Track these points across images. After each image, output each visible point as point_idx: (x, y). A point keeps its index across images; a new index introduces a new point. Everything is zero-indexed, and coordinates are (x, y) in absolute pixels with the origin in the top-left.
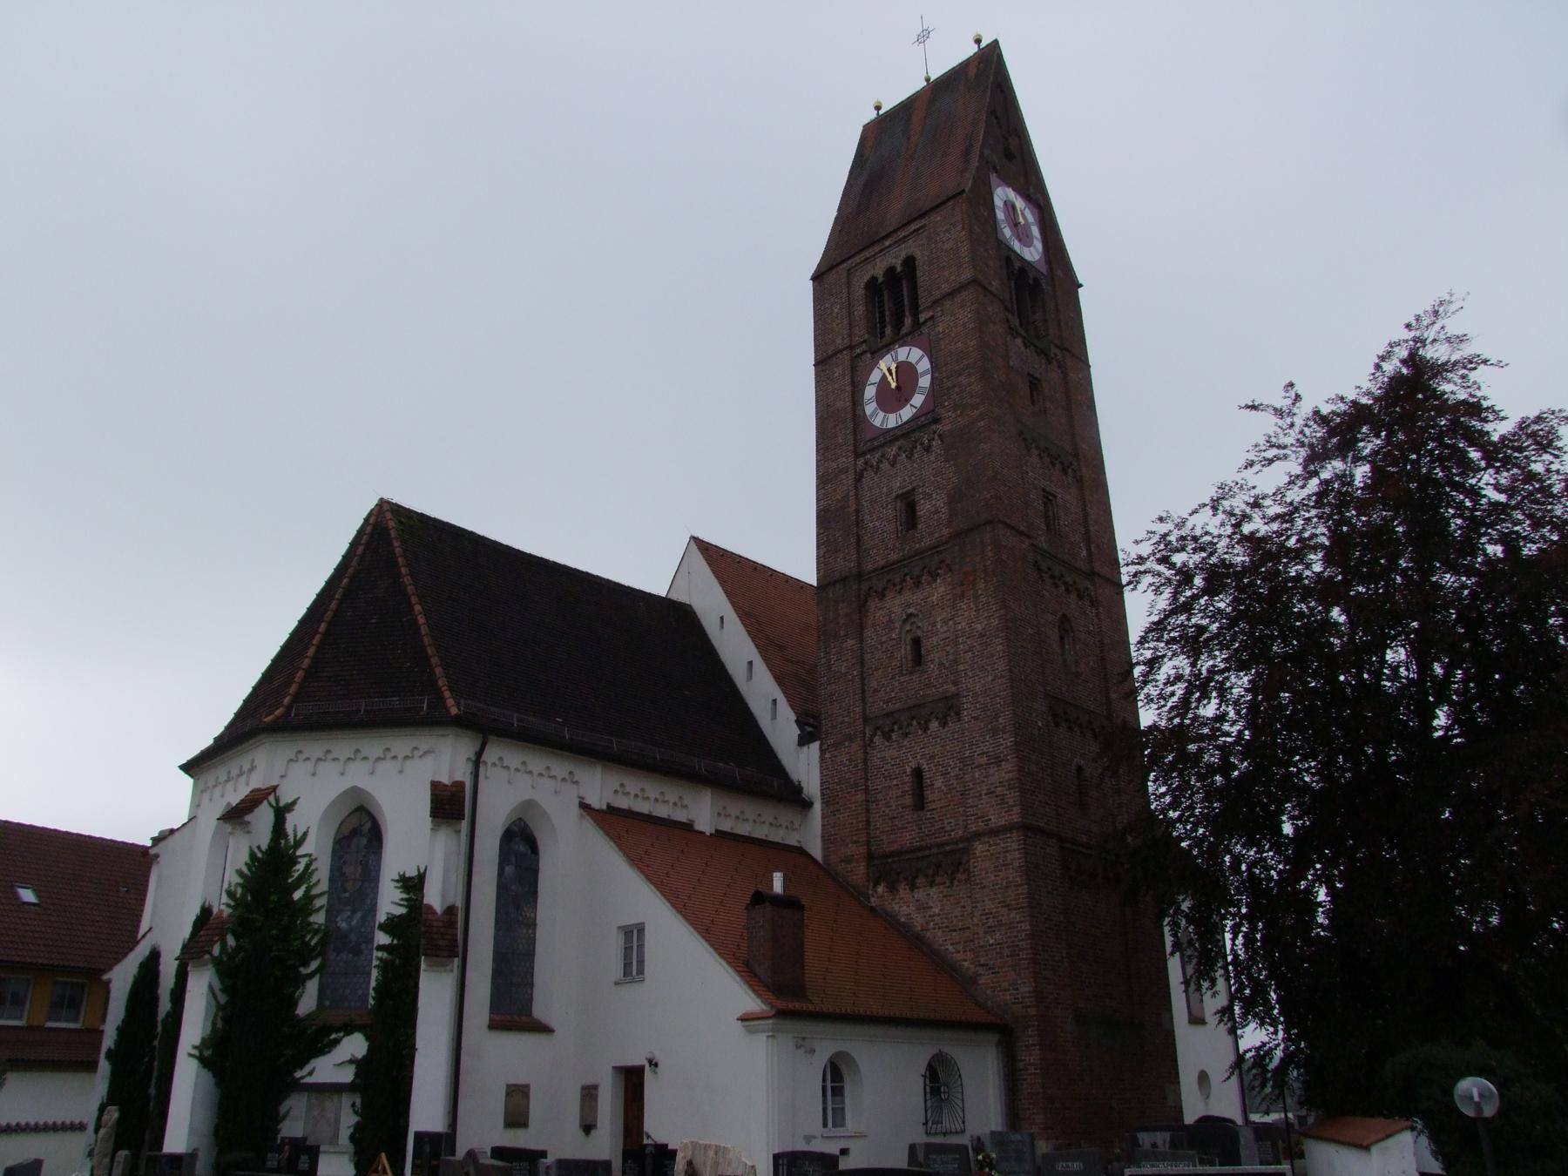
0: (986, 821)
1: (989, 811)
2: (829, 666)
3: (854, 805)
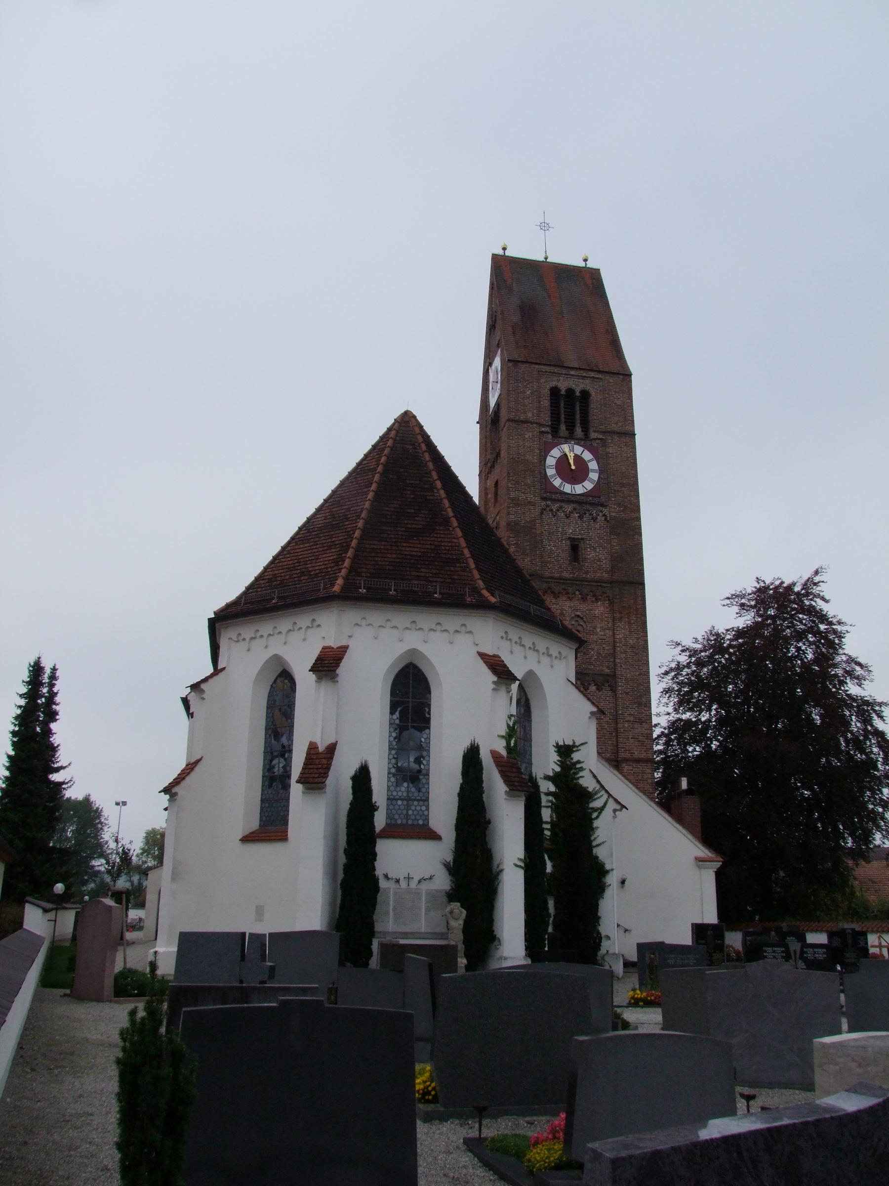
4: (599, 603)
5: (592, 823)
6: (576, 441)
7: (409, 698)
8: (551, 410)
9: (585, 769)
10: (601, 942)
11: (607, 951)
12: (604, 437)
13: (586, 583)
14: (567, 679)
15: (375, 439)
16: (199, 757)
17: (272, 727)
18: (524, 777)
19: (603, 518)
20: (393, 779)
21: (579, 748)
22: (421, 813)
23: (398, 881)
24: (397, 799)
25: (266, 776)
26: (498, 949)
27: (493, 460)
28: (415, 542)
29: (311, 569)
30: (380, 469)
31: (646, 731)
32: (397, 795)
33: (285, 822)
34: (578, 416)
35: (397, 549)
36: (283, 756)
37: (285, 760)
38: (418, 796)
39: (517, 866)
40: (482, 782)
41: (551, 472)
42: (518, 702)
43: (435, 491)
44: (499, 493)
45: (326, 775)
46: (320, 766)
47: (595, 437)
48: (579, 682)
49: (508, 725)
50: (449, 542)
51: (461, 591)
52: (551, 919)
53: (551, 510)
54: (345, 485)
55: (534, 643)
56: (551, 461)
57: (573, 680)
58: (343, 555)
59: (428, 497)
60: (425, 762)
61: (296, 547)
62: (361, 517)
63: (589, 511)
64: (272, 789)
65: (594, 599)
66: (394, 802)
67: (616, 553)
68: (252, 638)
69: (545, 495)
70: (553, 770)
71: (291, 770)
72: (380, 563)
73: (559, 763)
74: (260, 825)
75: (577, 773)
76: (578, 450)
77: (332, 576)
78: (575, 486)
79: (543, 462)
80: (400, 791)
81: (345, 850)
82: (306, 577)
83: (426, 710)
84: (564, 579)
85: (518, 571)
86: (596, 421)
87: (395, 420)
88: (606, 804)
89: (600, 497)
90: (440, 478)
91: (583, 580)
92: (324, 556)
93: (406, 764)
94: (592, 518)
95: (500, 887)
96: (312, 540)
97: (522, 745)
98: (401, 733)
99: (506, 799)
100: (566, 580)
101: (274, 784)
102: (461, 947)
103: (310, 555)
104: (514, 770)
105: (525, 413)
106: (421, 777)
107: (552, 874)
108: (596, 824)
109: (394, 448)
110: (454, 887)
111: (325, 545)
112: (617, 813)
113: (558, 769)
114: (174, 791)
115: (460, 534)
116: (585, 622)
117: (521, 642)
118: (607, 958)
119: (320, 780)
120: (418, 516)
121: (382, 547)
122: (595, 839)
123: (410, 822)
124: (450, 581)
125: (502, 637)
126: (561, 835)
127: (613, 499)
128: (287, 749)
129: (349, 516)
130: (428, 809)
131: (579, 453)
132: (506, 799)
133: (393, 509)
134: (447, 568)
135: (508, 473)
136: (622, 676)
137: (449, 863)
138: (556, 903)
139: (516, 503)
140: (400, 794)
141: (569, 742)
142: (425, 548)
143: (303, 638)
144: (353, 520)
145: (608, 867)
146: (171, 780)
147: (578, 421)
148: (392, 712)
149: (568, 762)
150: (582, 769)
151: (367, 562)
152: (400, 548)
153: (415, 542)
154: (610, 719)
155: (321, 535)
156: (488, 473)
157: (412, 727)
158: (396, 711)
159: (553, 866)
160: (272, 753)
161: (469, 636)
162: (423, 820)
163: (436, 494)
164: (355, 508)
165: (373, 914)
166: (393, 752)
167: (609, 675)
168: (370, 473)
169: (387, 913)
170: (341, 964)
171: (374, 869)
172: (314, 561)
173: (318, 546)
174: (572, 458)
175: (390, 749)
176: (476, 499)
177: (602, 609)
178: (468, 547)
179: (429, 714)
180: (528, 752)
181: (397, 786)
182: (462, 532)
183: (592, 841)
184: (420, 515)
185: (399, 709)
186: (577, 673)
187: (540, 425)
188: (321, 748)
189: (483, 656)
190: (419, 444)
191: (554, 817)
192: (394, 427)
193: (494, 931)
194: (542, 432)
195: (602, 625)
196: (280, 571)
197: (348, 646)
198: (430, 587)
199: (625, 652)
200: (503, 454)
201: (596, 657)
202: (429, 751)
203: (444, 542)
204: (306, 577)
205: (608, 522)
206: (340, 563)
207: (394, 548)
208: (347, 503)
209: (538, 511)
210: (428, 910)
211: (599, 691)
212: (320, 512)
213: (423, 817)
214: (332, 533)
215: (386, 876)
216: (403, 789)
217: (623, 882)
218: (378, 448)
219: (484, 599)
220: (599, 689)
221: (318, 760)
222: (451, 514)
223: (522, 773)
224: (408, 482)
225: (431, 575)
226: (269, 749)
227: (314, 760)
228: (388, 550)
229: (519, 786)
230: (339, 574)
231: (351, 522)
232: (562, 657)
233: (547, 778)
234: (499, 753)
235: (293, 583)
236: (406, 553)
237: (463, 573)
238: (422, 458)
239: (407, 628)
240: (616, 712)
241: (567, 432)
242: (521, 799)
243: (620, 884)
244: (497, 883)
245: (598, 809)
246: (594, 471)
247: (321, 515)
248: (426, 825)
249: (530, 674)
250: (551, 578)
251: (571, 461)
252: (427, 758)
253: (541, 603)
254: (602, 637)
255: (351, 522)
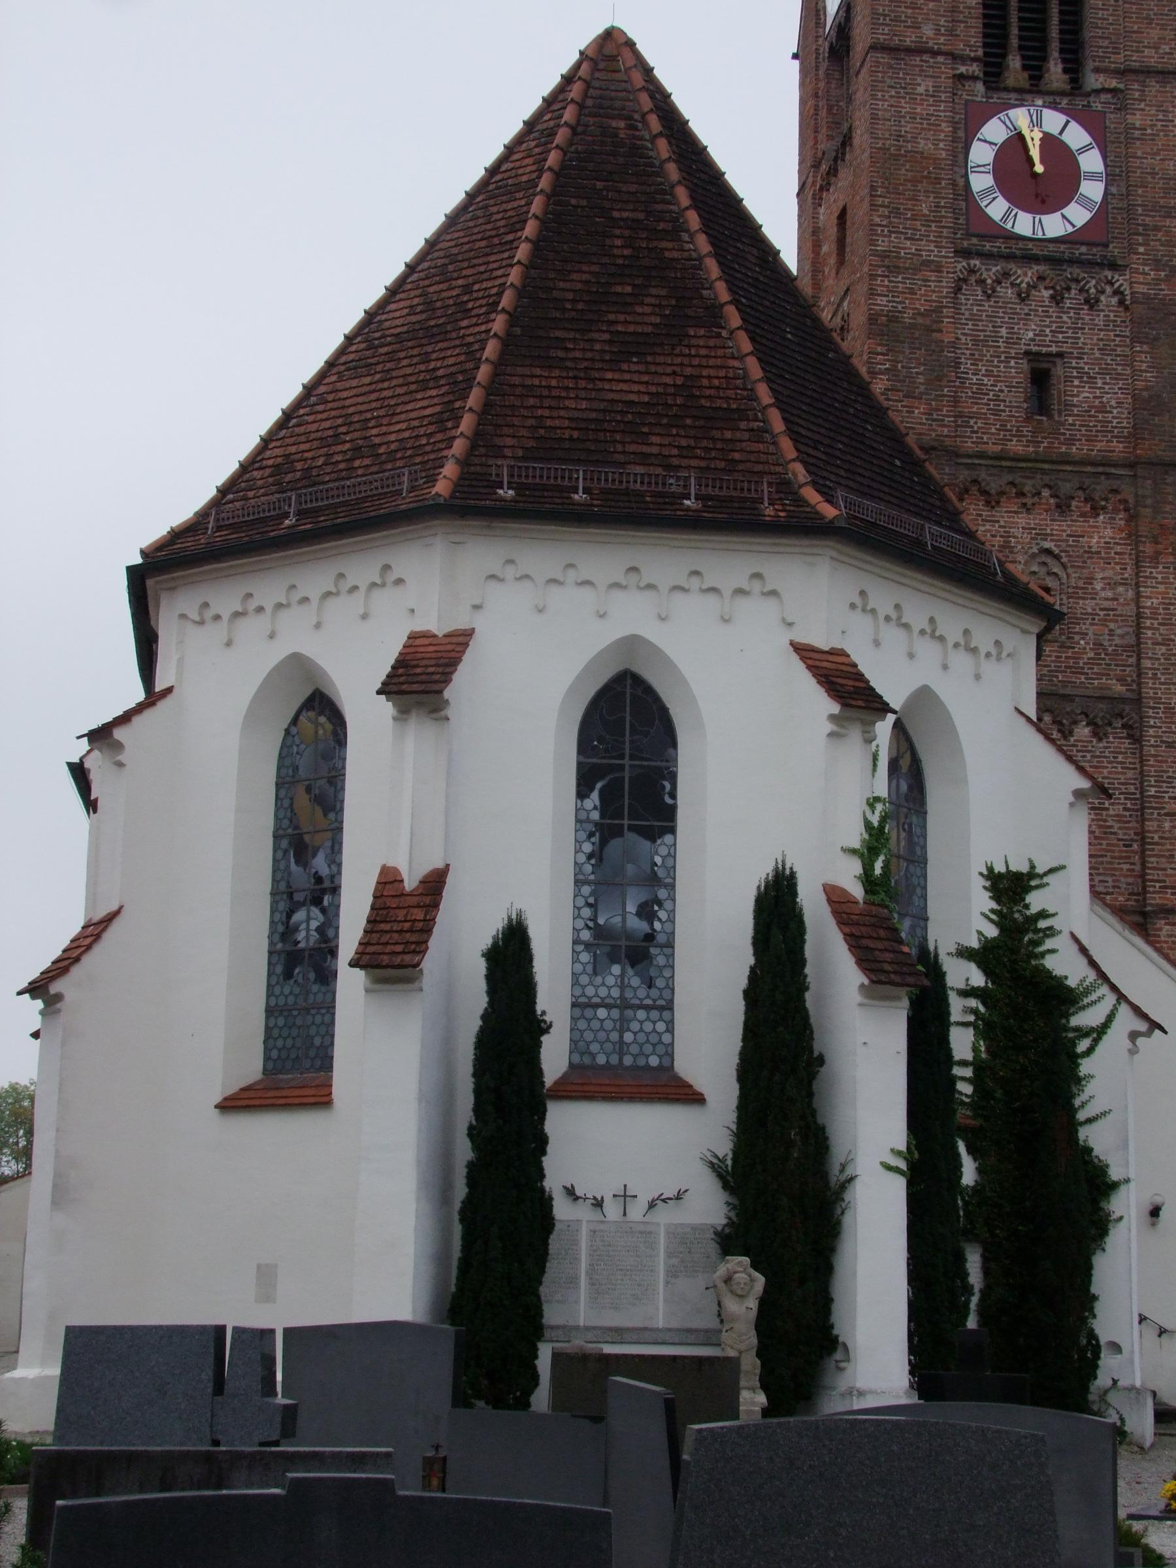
4: (1101, 517)
5: (1078, 1065)
6: (1049, 99)
7: (622, 757)
8: (985, 16)
9: (1060, 932)
10: (1099, 1358)
11: (1115, 1382)
12: (1121, 86)
13: (1069, 468)
14: (1016, 709)
15: (530, 105)
16: (115, 908)
17: (290, 831)
18: (906, 949)
19: (1114, 300)
20: (585, 957)
21: (1045, 880)
22: (654, 1038)
23: (598, 1204)
24: (596, 1006)
25: (279, 953)
26: (842, 1370)
27: (834, 154)
28: (634, 368)
29: (377, 440)
30: (545, 183)
32: (596, 995)
33: (326, 1063)
34: (1054, 32)
35: (590, 386)
36: (317, 901)
37: (324, 911)
38: (648, 996)
39: (889, 1168)
40: (802, 962)
41: (981, 182)
42: (894, 766)
43: (685, 236)
44: (848, 240)
45: (424, 946)
46: (407, 925)
47: (1098, 86)
48: (1047, 718)
49: (868, 825)
50: (722, 367)
51: (749, 490)
52: (975, 1300)
53: (981, 282)
54: (459, 227)
55: (932, 620)
56: (981, 154)
57: (1032, 712)
58: (458, 404)
59: (667, 254)
60: (662, 915)
61: (339, 386)
62: (500, 308)
63: (1077, 281)
64: (292, 982)
65: (1088, 509)
66: (589, 1013)
67: (1146, 389)
68: (237, 615)
69: (965, 244)
70: (979, 933)
71: (337, 936)
72: (549, 423)
73: (994, 917)
74: (265, 1070)
75: (1038, 943)
76: (1053, 121)
77: (432, 456)
78: (1044, 217)
79: (961, 157)
80: (603, 984)
81: (471, 1128)
82: (367, 462)
83: (664, 787)
84: (1012, 459)
85: (896, 438)
86: (1102, 43)
87: (581, 53)
88: (1110, 1018)
89: (1106, 246)
90: (697, 205)
91: (1066, 460)
92: (409, 407)
93: (617, 920)
94: (1087, 301)
95: (847, 1220)
96: (379, 368)
97: (902, 874)
98: (603, 843)
99: (860, 1005)
100: (1019, 460)
101: (297, 971)
102: (751, 1364)
103: (374, 405)
104: (882, 933)
105: (916, 26)
106: (653, 951)
107: (977, 1189)
108: (1086, 1067)
109: (580, 129)
110: (735, 1219)
111: (412, 379)
112: (1140, 1041)
113: (992, 932)
114: (54, 988)
115: (746, 346)
116: (1064, 566)
117: (899, 618)
118: (1112, 1398)
119: (407, 958)
120: (642, 304)
121: (554, 383)
122: (1083, 1105)
123: (628, 1061)
124: (722, 465)
125: (853, 606)
126: (999, 1094)
127: (1141, 249)
128: (327, 884)
129: (470, 305)
130: (670, 1030)
131: (1055, 131)
132: (860, 1005)
133: (579, 286)
134: (716, 434)
135: (873, 188)
136: (1157, 700)
137: (723, 1161)
138: (986, 1260)
139: (890, 263)
140: (603, 992)
141: (1019, 865)
142: (658, 384)
143: (361, 612)
144: (478, 316)
145: (1115, 1174)
146: (46, 964)
147: (1054, 47)
148: (582, 792)
149: (1017, 915)
150: (1051, 932)
151: (516, 421)
152: (600, 385)
153: (634, 368)
154: (1125, 809)
155: (402, 355)
156: (821, 189)
157: (632, 828)
158: (592, 789)
159: (980, 1171)
160: (290, 895)
161: (772, 603)
162: (660, 1057)
163: (687, 246)
164: (484, 285)
165: (540, 1283)
166: (586, 890)
167: (1123, 700)
168: (521, 195)
169: (573, 1281)
170: (460, 1400)
171: (541, 1176)
172: (385, 421)
173: (394, 382)
174: (1037, 142)
175: (578, 883)
176: (790, 258)
177: (1108, 532)
178: (768, 380)
179: (673, 796)
180: (918, 891)
181: (595, 973)
182: (752, 339)
183: (1075, 1111)
184: (647, 300)
185: (599, 785)
186: (1040, 695)
187: (954, 57)
188: (410, 883)
189: (804, 653)
190: (644, 115)
191: (983, 1049)
192: (581, 73)
193: (832, 1327)
194: (961, 78)
196: (303, 447)
197: (473, 630)
198: (671, 481)
200: (860, 138)
201: (1091, 655)
202: (672, 887)
203: (708, 367)
204: (367, 462)
205: (1127, 308)
206: (449, 424)
207: (582, 384)
208: (464, 273)
209: (947, 284)
210: (672, 1273)
211: (1100, 740)
212: (398, 297)
213: (661, 1049)
214: (429, 349)
215: (570, 1192)
216: (610, 981)
217: (1155, 1212)
218: (540, 127)
219: (808, 510)
220: (1098, 734)
221: (404, 912)
222: (724, 295)
223: (901, 942)
224: (616, 214)
225: (675, 452)
226: (283, 886)
227: (392, 912)
228: (567, 388)
229: (895, 973)
230: (445, 453)
231: (474, 320)
232: (1004, 655)
233: (965, 953)
234: (844, 892)
235: (334, 476)
236: (611, 396)
237: (755, 447)
238: (651, 154)
239: (616, 585)
240: (1141, 793)
241: (1026, 75)
242: (899, 1004)
243: (1149, 1219)
244: (839, 1211)
245: (1092, 1030)
246: (1092, 176)
247: (401, 305)
248: (667, 1068)
249: (924, 697)
250: (982, 455)
251: (1035, 153)
252: (668, 905)
253: (952, 519)
254: (1106, 604)
255: (474, 320)
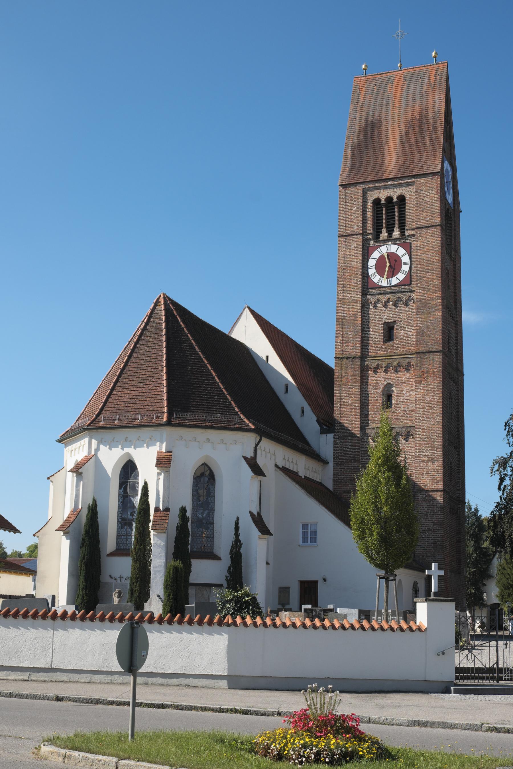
0: (425, 485)
1: (427, 481)
2: (341, 399)
3: (352, 467)
31: (437, 468)
154: (411, 460)
195: (408, 388)
199: (423, 408)
